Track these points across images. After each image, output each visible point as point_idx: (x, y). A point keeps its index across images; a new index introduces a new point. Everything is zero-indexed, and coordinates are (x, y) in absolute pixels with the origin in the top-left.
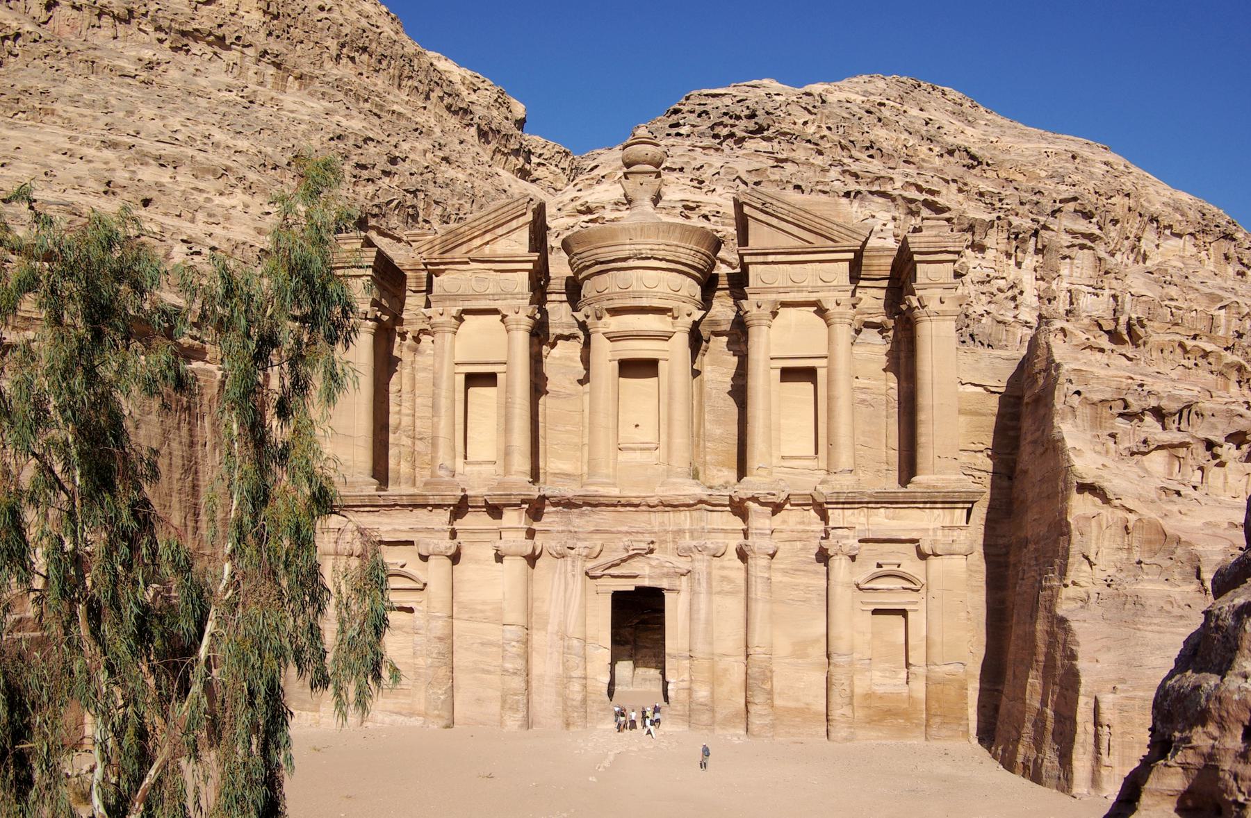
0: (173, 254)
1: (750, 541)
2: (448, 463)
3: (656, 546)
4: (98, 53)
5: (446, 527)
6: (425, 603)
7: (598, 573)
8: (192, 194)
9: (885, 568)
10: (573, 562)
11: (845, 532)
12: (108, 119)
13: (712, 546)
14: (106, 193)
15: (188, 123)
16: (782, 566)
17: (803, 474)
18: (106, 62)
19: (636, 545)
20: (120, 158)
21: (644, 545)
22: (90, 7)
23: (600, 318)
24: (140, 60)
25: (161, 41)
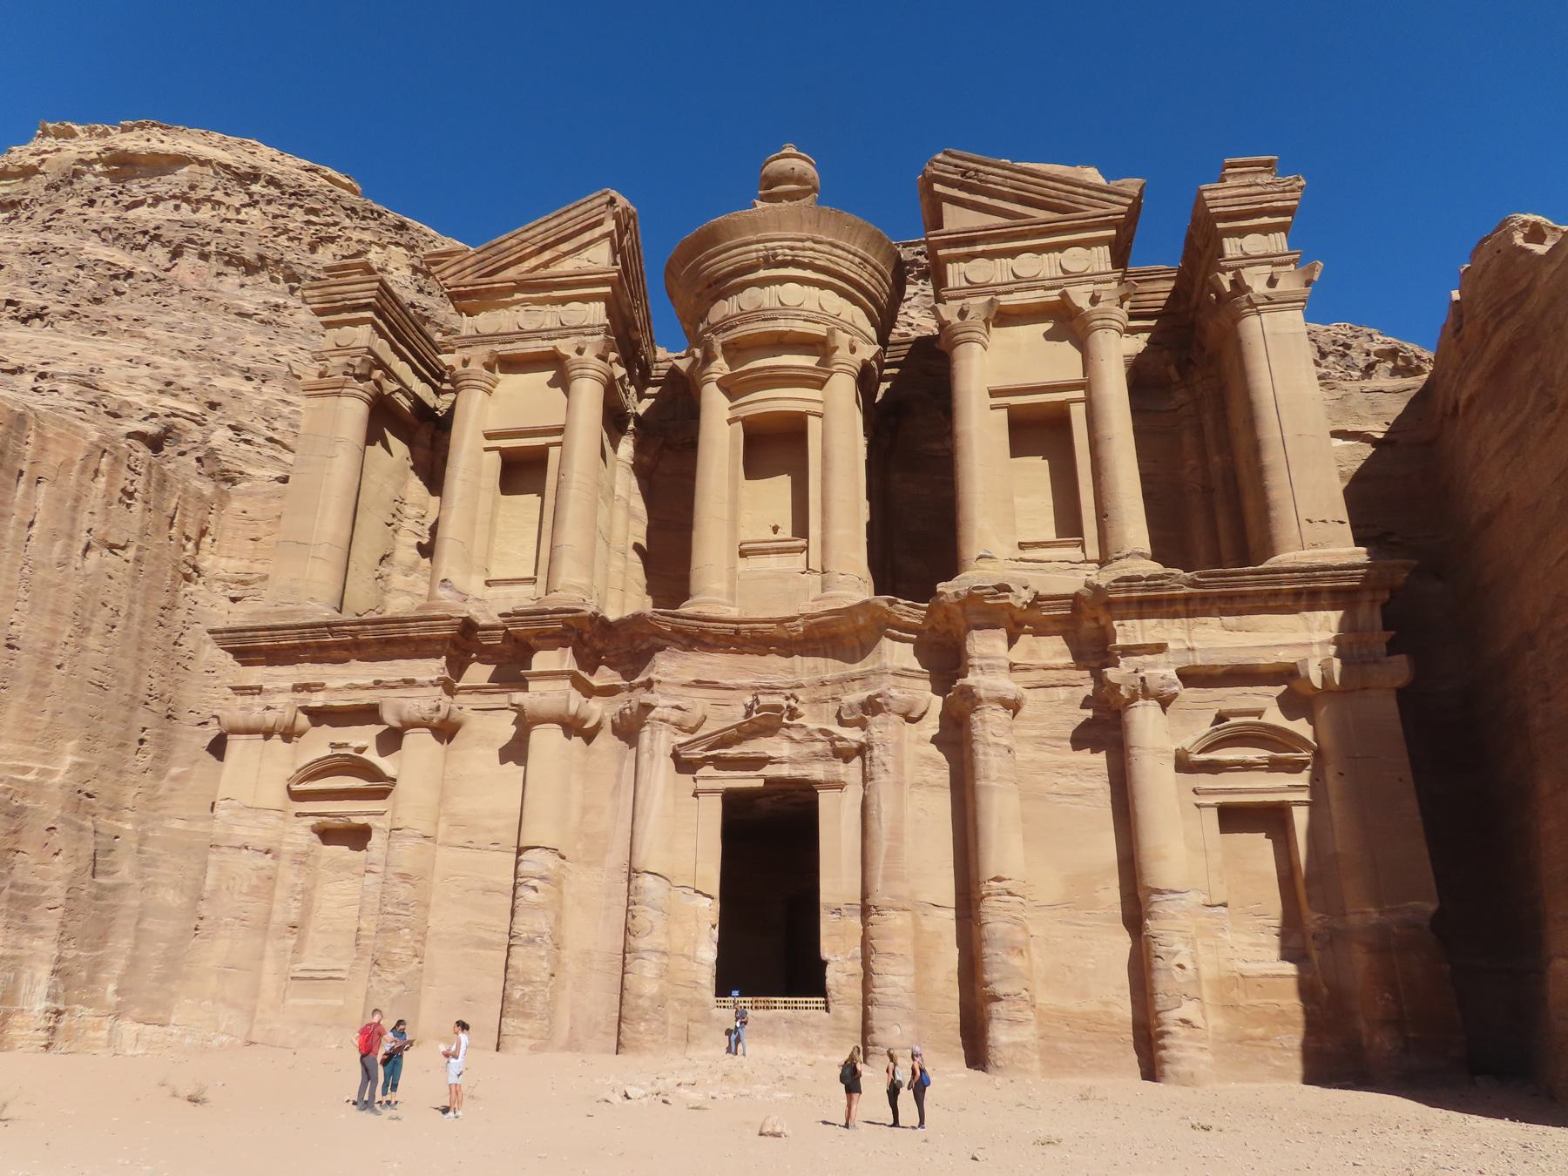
0: (211, 437)
1: (970, 679)
2: (457, 579)
3: (801, 709)
4: (217, 294)
5: (434, 678)
6: (388, 816)
7: (697, 753)
8: (276, 405)
9: (1233, 721)
10: (652, 733)
11: (1149, 658)
12: (203, 342)
13: (902, 696)
14: (161, 392)
15: (299, 351)
16: (1034, 733)
17: (1059, 570)
18: (222, 301)
19: (764, 700)
20: (195, 367)
21: (777, 700)
22: (219, 253)
23: (708, 358)
24: (265, 303)
25: (292, 290)
